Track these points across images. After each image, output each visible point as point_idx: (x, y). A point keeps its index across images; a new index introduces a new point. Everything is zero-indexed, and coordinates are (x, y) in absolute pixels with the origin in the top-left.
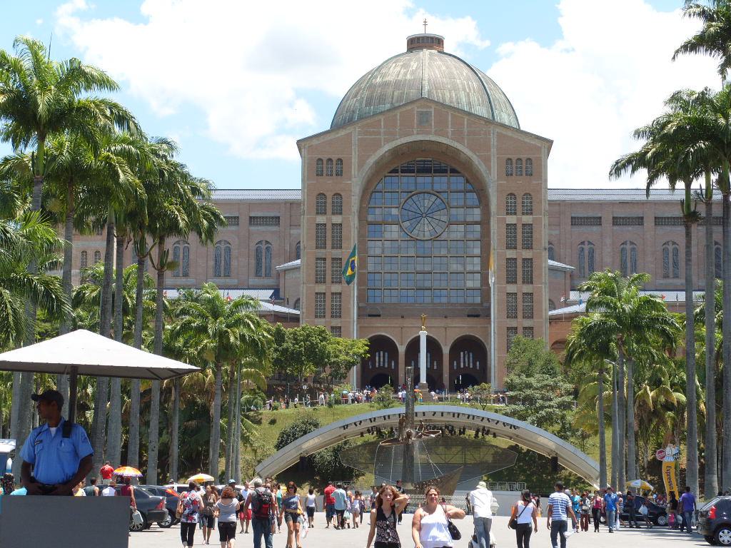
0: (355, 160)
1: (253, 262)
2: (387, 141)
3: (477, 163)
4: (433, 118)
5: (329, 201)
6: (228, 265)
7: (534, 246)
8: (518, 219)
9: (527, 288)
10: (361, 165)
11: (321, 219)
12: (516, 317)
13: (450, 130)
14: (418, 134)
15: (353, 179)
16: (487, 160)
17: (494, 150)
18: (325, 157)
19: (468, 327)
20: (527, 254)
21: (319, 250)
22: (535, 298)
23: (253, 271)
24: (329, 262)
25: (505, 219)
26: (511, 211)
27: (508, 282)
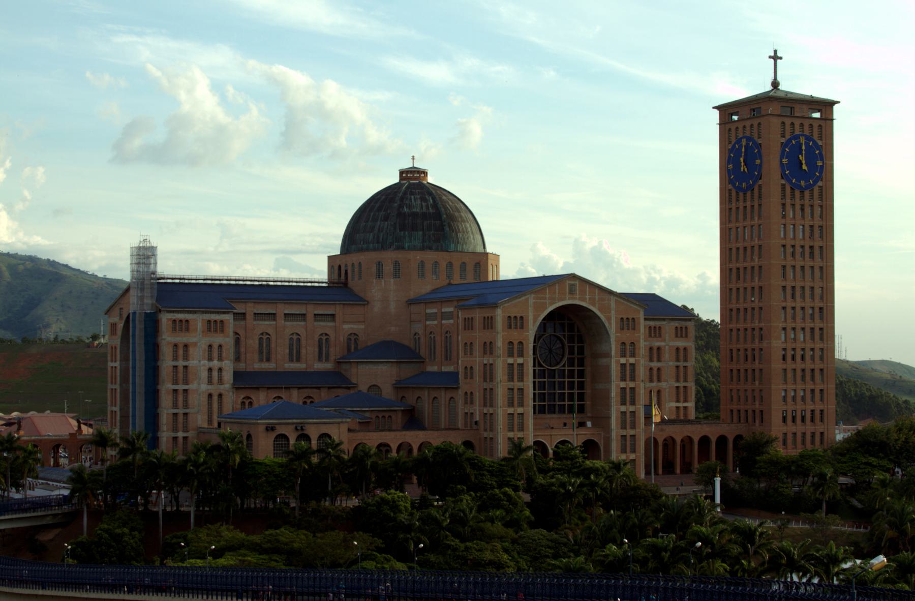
0: (531, 318)
1: (317, 350)
2: (551, 304)
3: (603, 320)
4: (578, 288)
5: (516, 347)
6: (299, 352)
7: (636, 379)
8: (627, 360)
9: (632, 408)
10: (534, 322)
11: (510, 361)
12: (625, 428)
13: (587, 297)
14: (569, 299)
15: (530, 332)
16: (609, 319)
17: (613, 312)
18: (512, 315)
19: (590, 434)
20: (632, 385)
21: (509, 383)
22: (637, 415)
23: (317, 358)
24: (516, 391)
25: (619, 360)
26: (623, 355)
27: (621, 404)
